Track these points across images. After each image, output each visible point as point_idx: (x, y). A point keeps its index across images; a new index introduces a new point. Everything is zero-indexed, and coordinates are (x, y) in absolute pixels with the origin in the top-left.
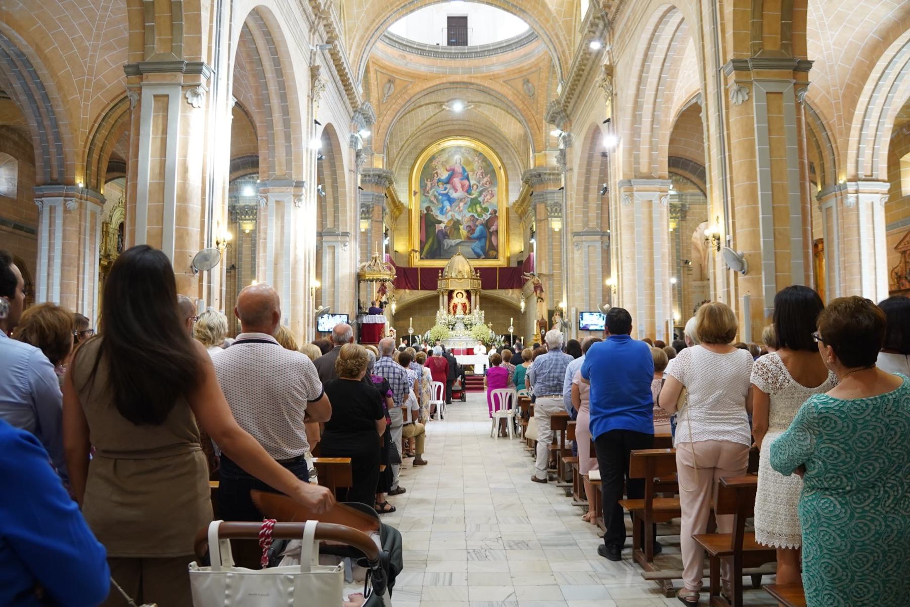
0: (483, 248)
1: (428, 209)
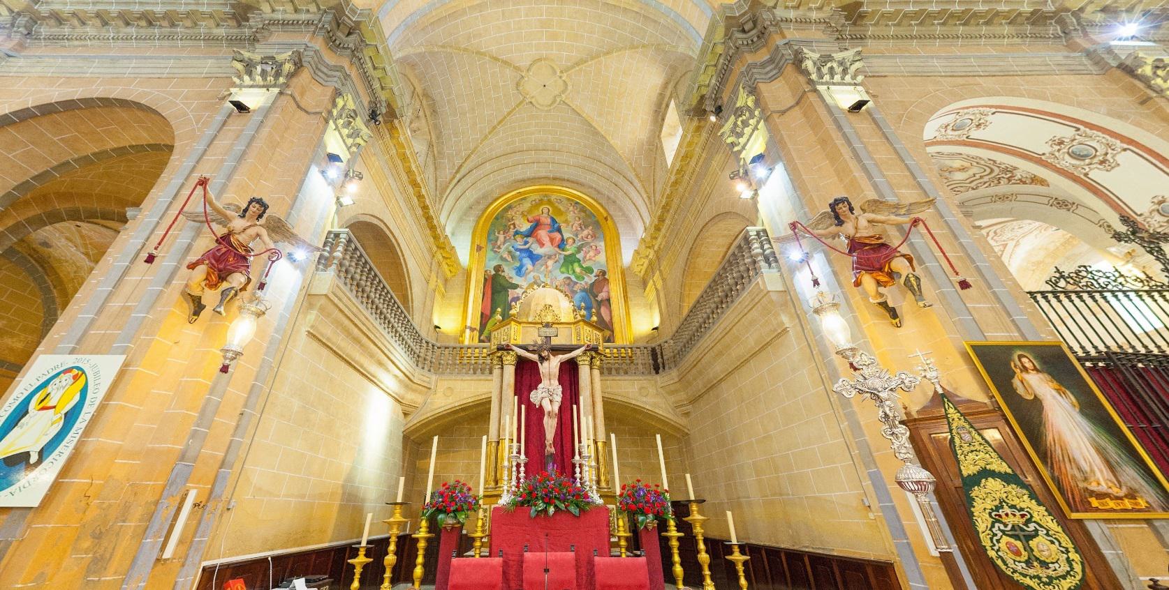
1: (498, 268)
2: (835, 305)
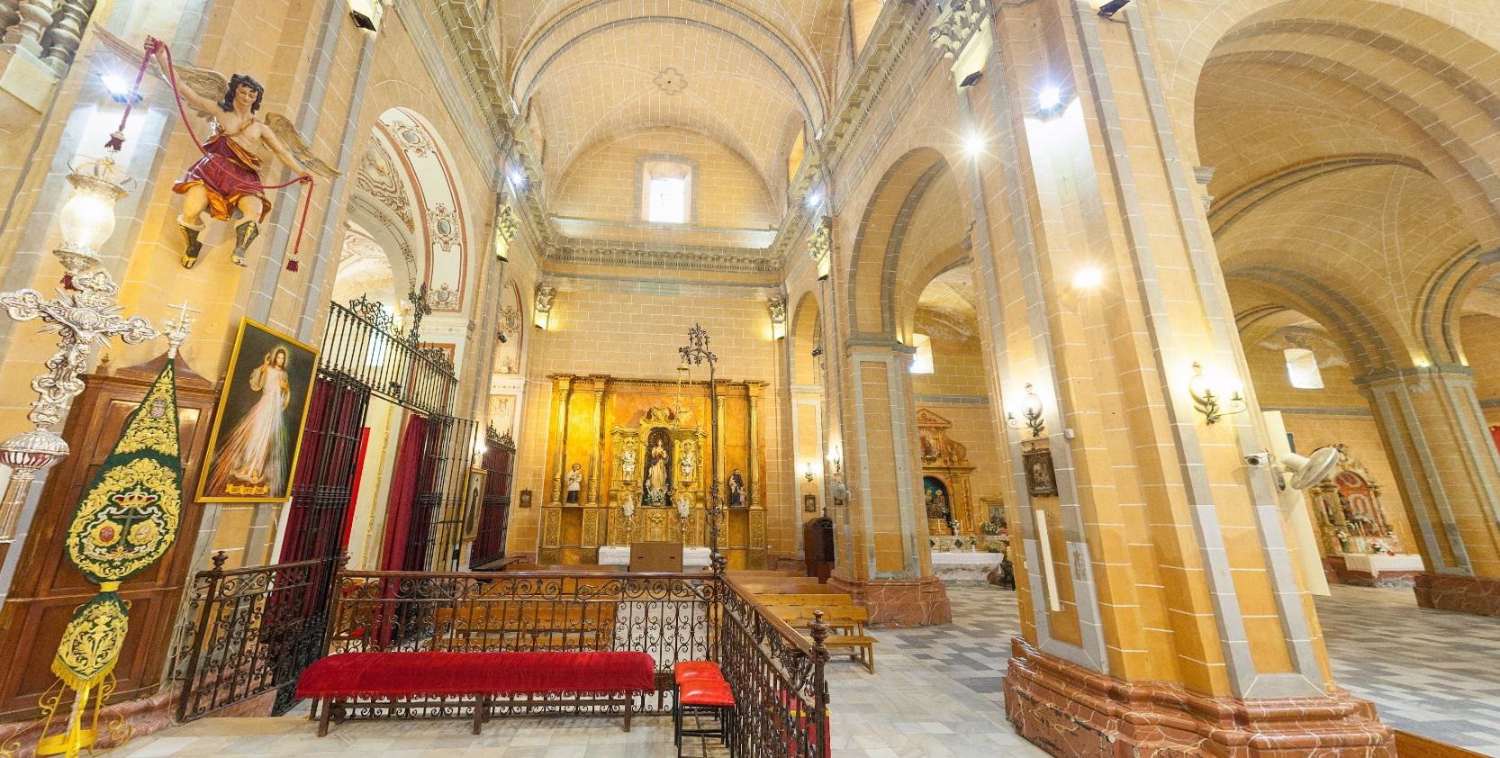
2: (118, 191)
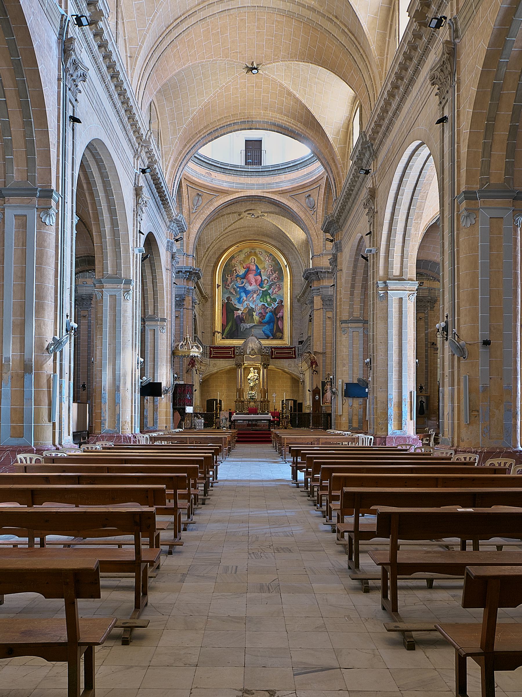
0: (271, 331)
1: (228, 299)
